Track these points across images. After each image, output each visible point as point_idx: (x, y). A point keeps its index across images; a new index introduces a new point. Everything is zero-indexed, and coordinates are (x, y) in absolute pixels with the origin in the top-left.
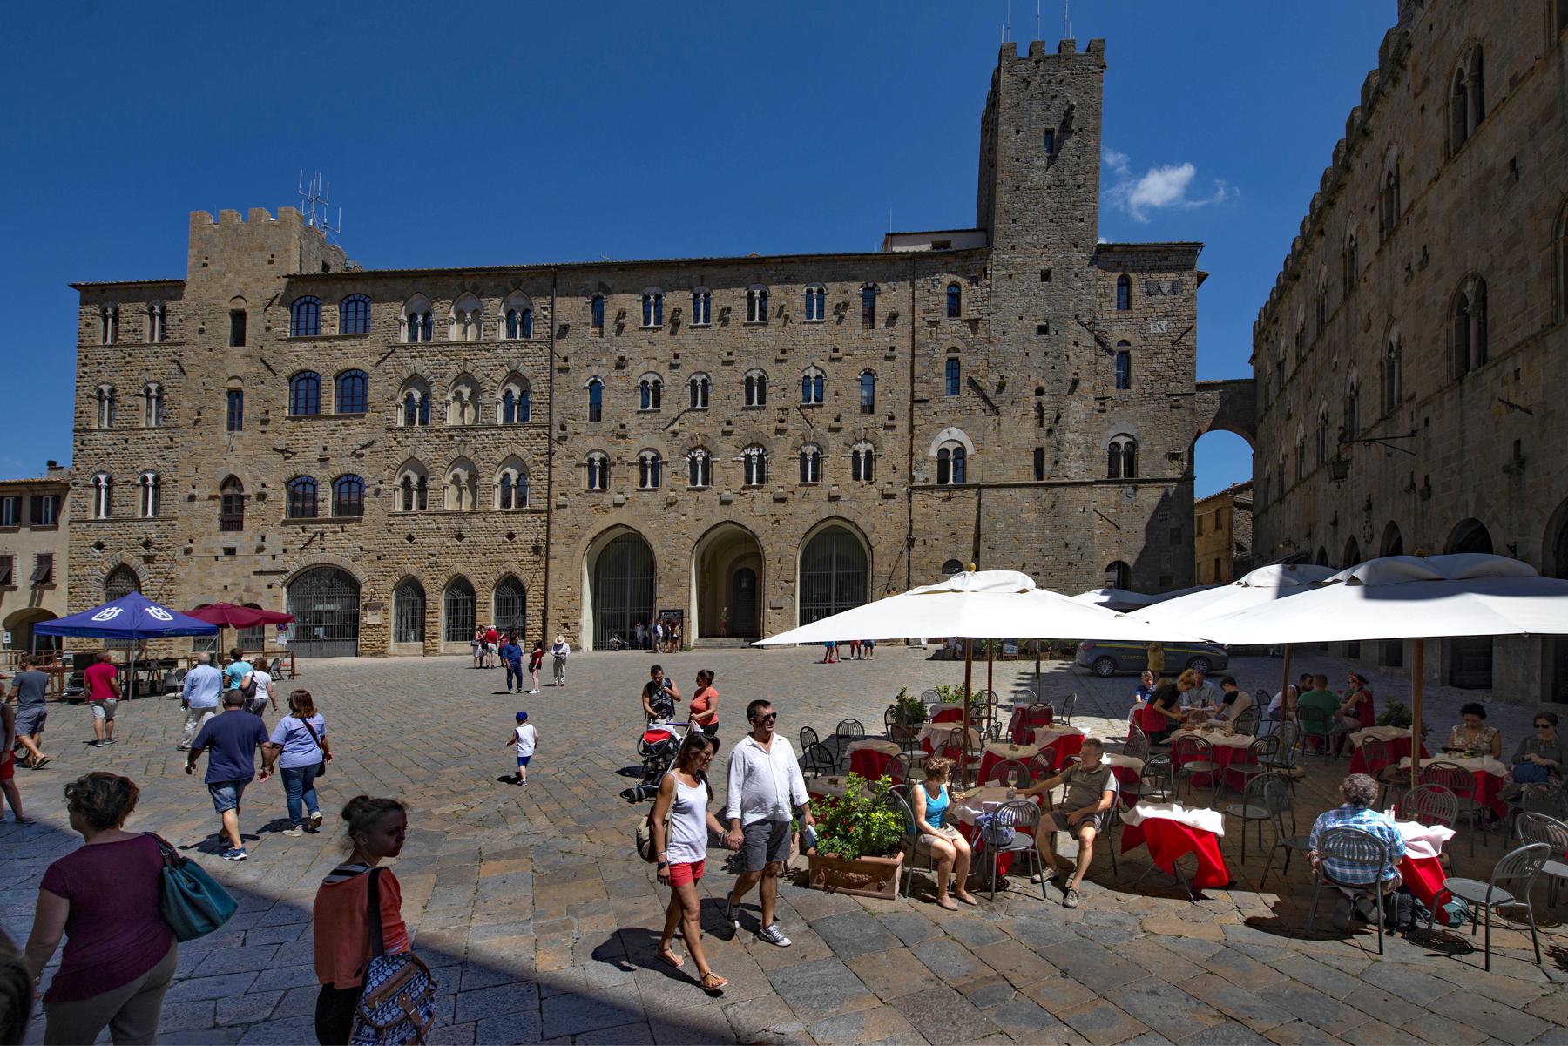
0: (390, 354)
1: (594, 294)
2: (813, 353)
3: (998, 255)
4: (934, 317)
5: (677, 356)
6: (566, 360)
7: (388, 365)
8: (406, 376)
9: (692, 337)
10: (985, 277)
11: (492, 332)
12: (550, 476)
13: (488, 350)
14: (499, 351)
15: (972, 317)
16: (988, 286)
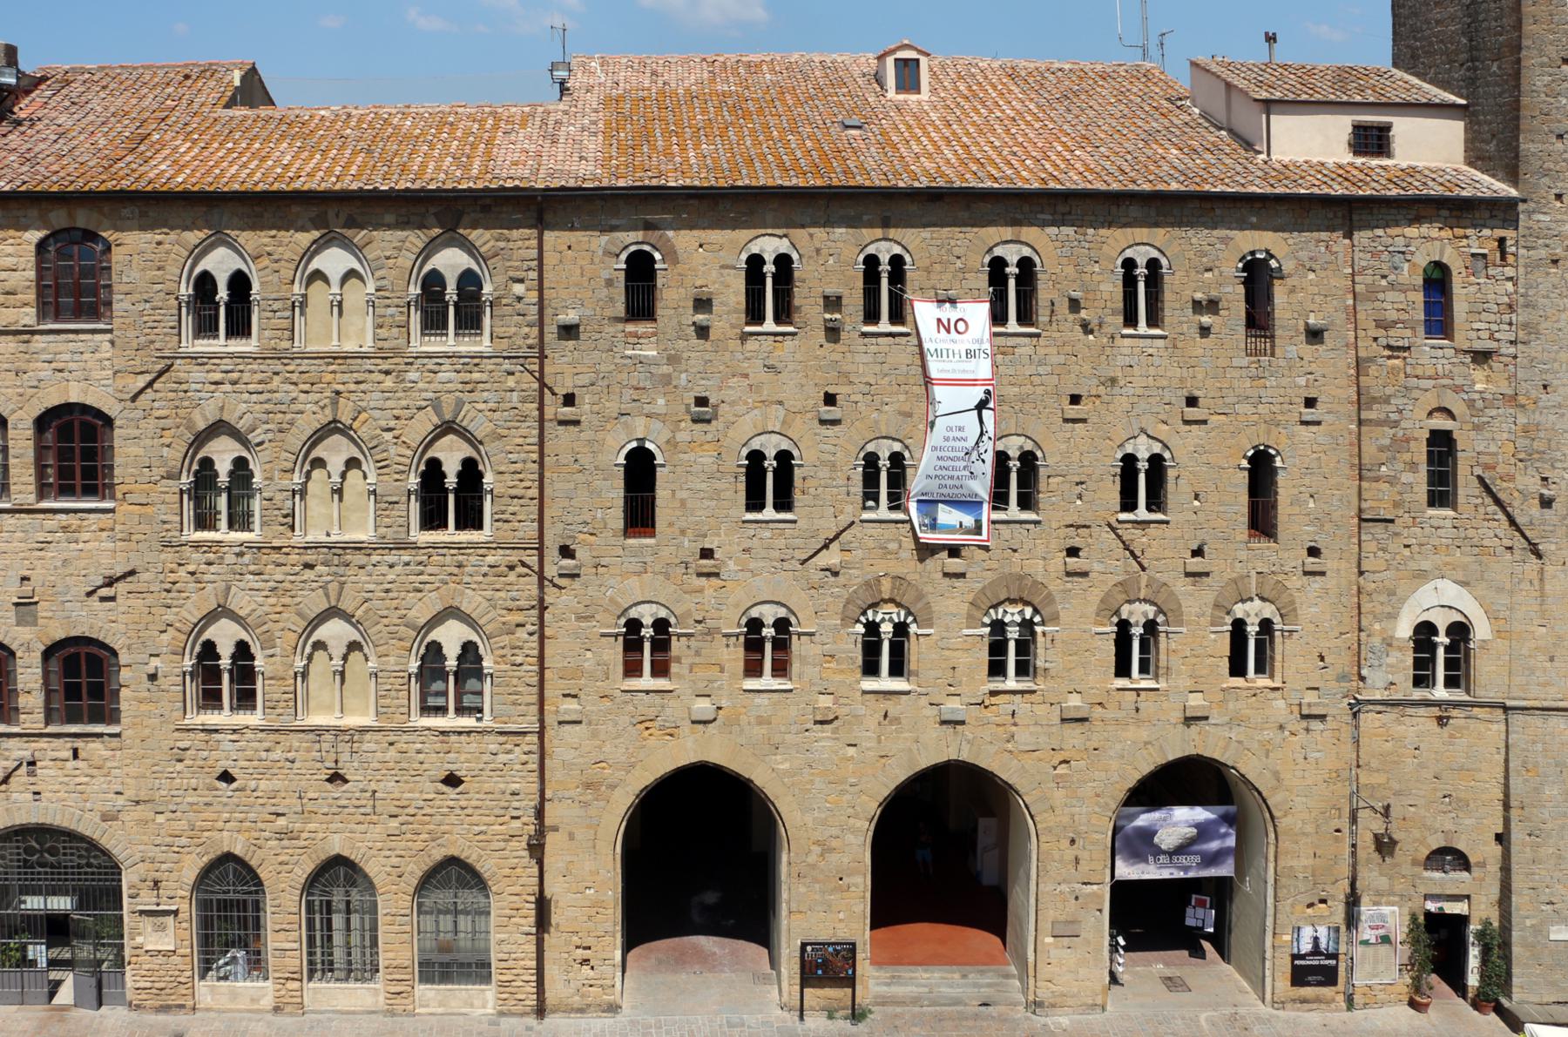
0: (161, 374)
1: (633, 248)
2: (1142, 405)
3: (1530, 213)
4: (1399, 336)
5: (830, 399)
6: (569, 400)
7: (160, 399)
8: (201, 425)
9: (866, 359)
10: (1503, 258)
11: (395, 330)
12: (541, 658)
13: (387, 373)
14: (413, 375)
15: (1479, 346)
16: (1510, 279)
